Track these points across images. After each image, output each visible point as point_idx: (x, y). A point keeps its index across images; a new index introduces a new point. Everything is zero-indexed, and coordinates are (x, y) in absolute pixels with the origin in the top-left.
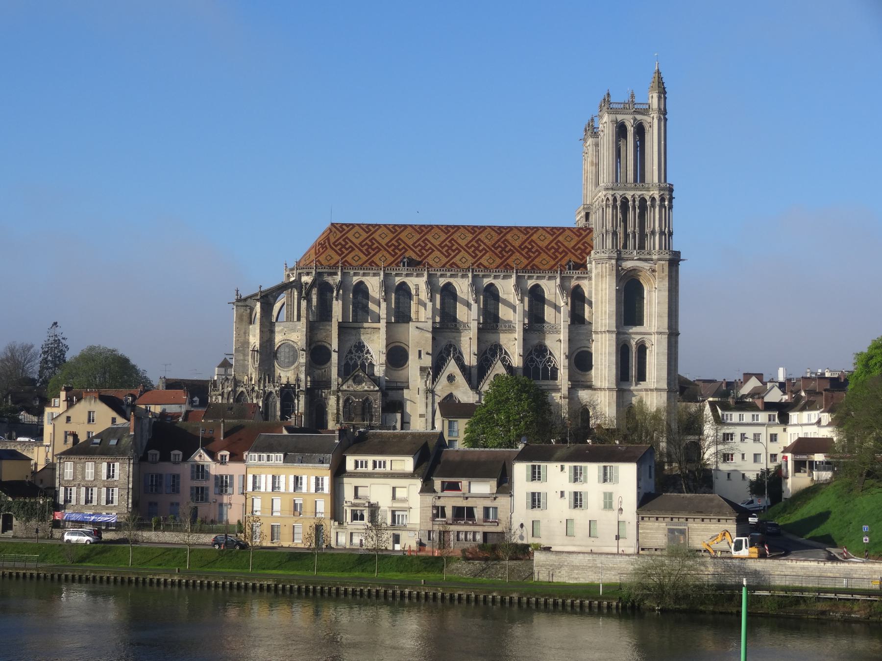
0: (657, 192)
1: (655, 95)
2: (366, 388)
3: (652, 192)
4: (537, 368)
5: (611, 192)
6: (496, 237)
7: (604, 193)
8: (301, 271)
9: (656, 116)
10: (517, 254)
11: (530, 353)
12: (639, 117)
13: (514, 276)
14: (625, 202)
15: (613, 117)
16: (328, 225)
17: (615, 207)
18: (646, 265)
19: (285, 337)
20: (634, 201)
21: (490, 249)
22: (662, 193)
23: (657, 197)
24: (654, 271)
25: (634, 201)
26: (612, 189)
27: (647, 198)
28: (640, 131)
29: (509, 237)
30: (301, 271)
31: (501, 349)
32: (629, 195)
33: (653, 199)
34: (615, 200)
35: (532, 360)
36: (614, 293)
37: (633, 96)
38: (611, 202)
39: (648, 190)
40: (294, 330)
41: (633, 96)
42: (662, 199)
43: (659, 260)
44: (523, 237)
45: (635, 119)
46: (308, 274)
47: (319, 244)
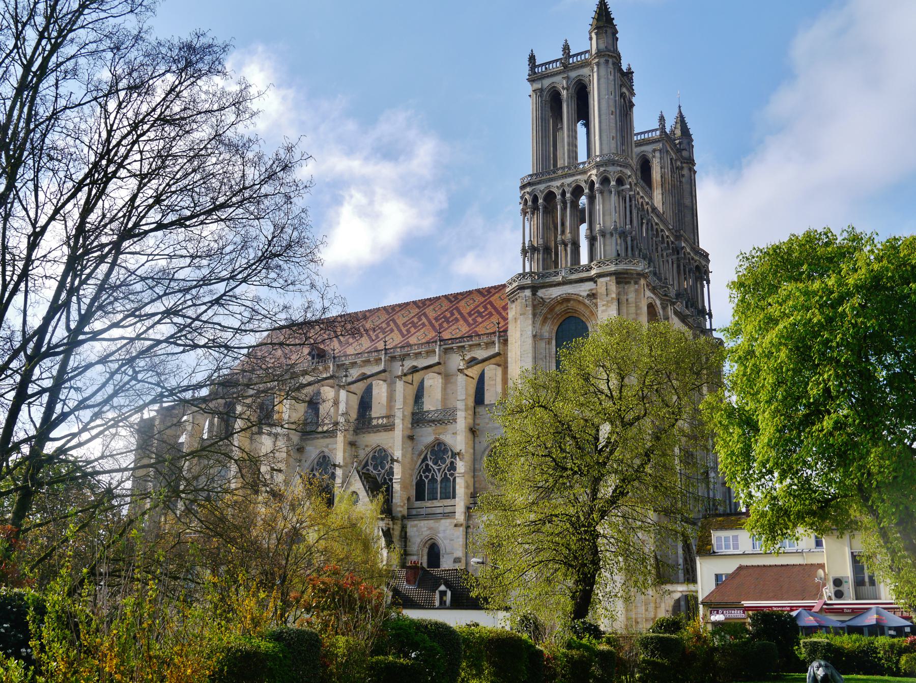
0: (594, 172)
4: (433, 480)
5: (528, 189)
6: (446, 305)
10: (461, 322)
11: (425, 459)
12: (573, 74)
13: (437, 350)
14: (550, 196)
15: (538, 85)
17: (535, 208)
18: (583, 289)
20: (563, 194)
21: (430, 322)
22: (602, 169)
23: (594, 178)
25: (563, 194)
26: (529, 184)
27: (583, 185)
28: (581, 93)
29: (462, 303)
31: (386, 456)
32: (555, 186)
33: (592, 183)
34: (535, 199)
35: (427, 469)
36: (530, 341)
37: (566, 48)
38: (530, 203)
41: (566, 48)
42: (605, 181)
43: (600, 275)
44: (479, 299)
45: (568, 78)
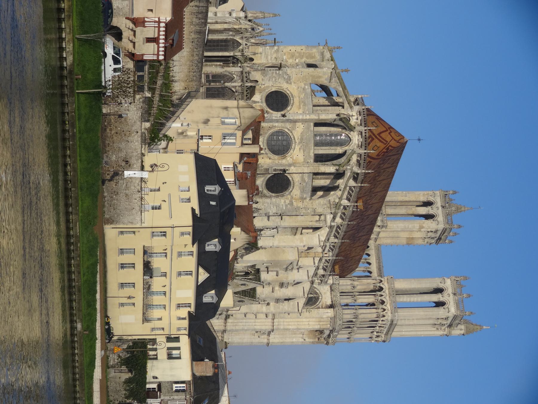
0: (383, 339)
1: (462, 332)
2: (239, 253)
3: (383, 336)
5: (389, 323)
7: (390, 318)
8: (363, 157)
9: (445, 333)
16: (407, 138)
19: (297, 184)
24: (319, 339)
30: (363, 157)
39: (387, 334)
40: (303, 191)
46: (358, 161)
47: (388, 149)
